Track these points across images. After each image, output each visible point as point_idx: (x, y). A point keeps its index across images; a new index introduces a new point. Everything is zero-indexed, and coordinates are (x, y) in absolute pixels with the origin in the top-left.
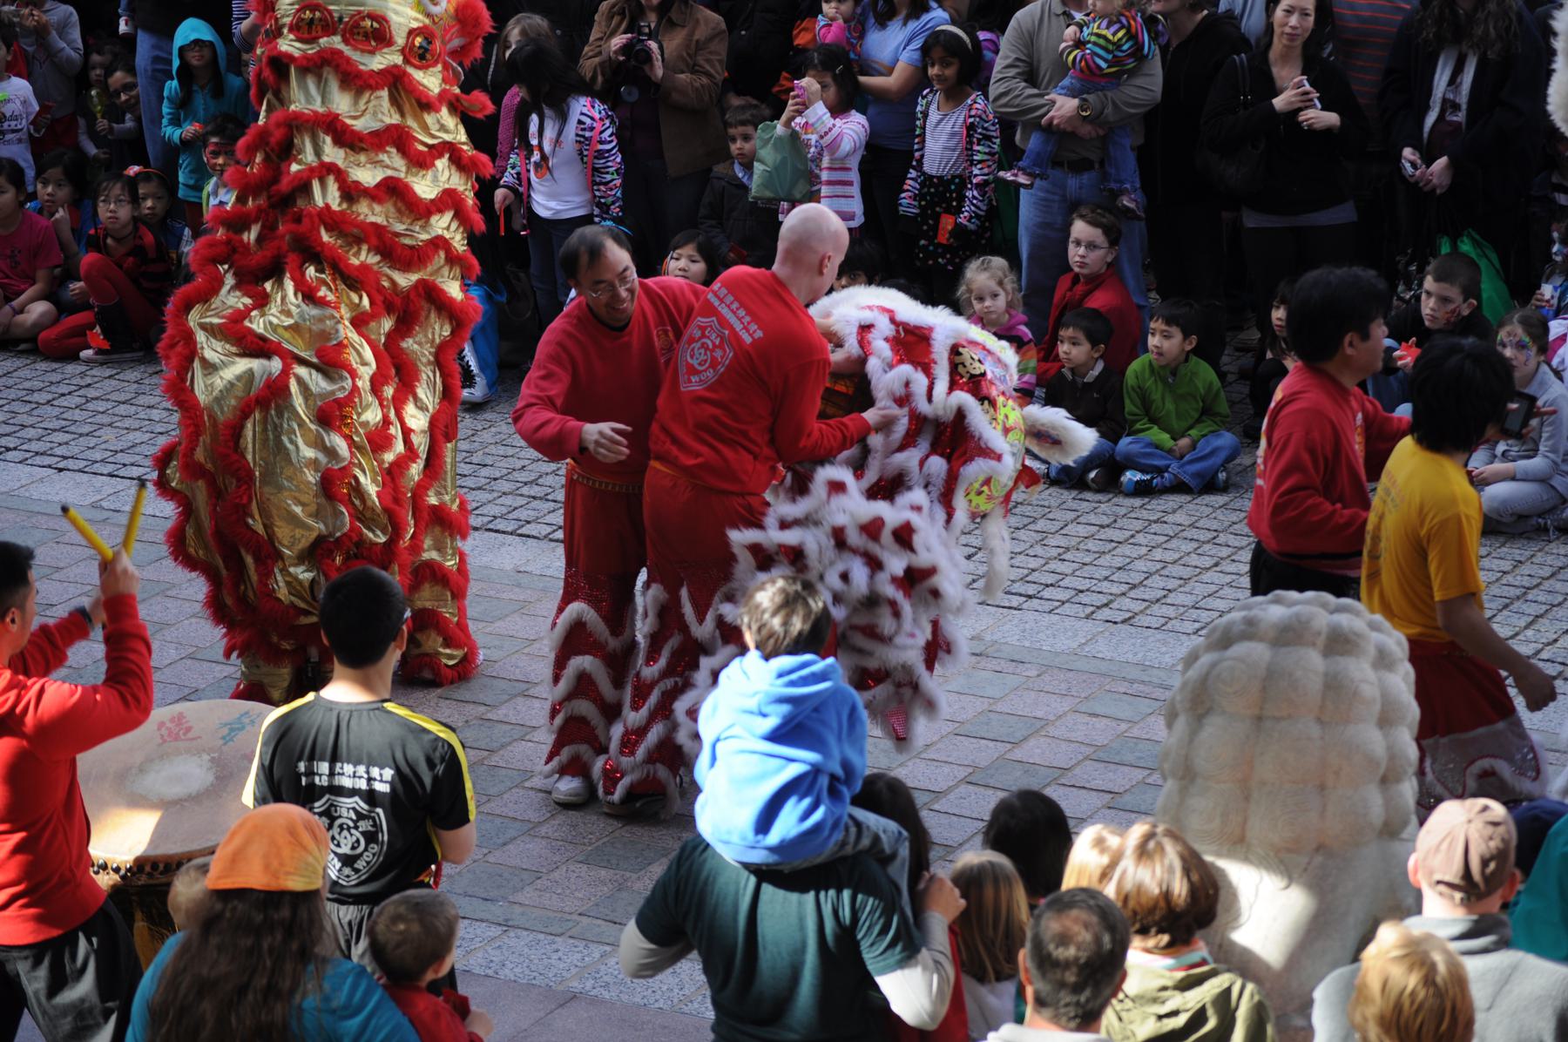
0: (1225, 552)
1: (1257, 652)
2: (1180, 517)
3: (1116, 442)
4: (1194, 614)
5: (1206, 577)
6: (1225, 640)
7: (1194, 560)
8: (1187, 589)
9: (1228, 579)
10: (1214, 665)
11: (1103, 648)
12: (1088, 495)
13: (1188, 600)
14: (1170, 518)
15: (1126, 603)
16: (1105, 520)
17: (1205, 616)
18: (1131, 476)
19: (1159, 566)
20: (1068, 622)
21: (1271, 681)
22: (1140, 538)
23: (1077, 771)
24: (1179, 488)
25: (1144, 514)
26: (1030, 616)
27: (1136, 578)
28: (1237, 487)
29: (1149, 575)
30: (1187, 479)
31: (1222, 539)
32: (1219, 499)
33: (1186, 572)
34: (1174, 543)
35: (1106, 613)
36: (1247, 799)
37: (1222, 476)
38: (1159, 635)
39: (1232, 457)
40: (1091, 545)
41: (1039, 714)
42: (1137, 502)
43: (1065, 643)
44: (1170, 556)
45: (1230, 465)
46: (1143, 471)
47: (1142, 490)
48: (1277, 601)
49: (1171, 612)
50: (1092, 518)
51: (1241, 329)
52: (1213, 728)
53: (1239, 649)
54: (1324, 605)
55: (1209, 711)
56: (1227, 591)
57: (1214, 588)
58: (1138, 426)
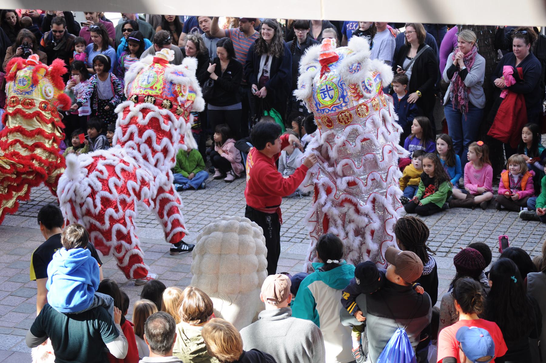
0: (206, 207)
1: (219, 234)
2: (192, 197)
4: (197, 226)
5: (200, 214)
7: (196, 210)
8: (195, 218)
9: (207, 215)
10: (206, 239)
13: (196, 222)
14: (188, 198)
17: (201, 226)
19: (186, 212)
21: (223, 244)
23: (165, 275)
24: (191, 188)
26: (148, 229)
28: (208, 187)
30: (193, 186)
31: (204, 203)
33: (194, 213)
34: (190, 205)
36: (218, 279)
37: (203, 184)
39: (206, 179)
41: (153, 258)
44: (189, 209)
45: (206, 181)
46: (180, 184)
48: (224, 219)
51: (207, 140)
52: (206, 258)
53: (213, 234)
54: (238, 220)
56: (207, 218)
57: (203, 218)
58: (178, 171)
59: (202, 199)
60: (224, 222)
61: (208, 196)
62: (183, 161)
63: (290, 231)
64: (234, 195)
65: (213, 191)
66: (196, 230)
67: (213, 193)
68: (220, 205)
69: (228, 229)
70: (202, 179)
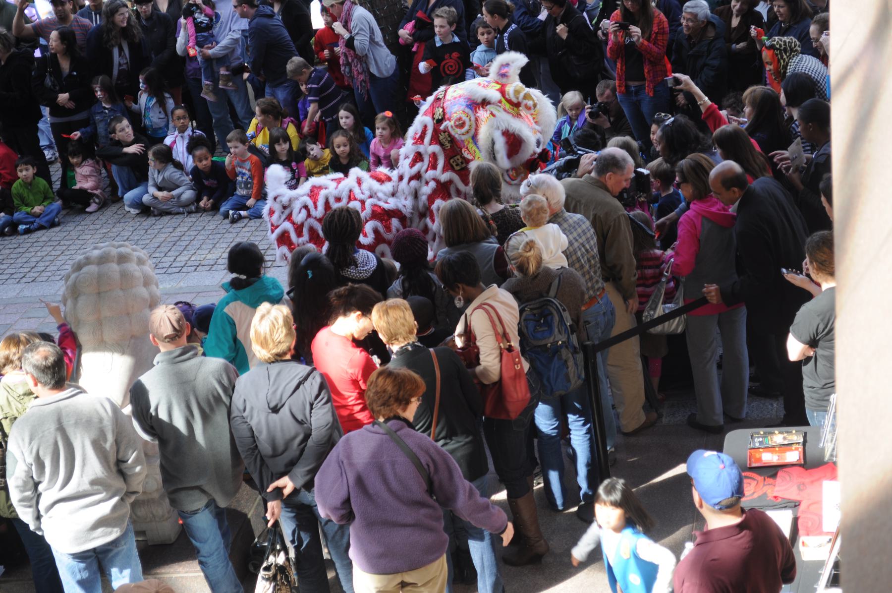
0: (64, 248)
1: (92, 268)
2: (44, 238)
3: (12, 215)
4: (59, 273)
5: (60, 258)
6: (79, 267)
10: (77, 277)
11: (27, 293)
12: (6, 238)
13: (55, 268)
14: (40, 240)
15: (31, 274)
16: (16, 246)
17: (63, 273)
18: (21, 227)
20: (10, 286)
21: (100, 278)
22: (31, 249)
24: (41, 228)
25: (30, 240)
27: (33, 264)
28: (63, 223)
29: (38, 262)
30: (43, 224)
31: (62, 243)
32: (57, 229)
33: (52, 258)
34: (44, 249)
35: (24, 280)
36: (101, 324)
37: (57, 220)
38: (47, 283)
40: (12, 256)
42: (26, 236)
43: (12, 294)
44: (44, 254)
47: (27, 232)
48: (95, 248)
49: (49, 274)
50: (10, 246)
52: (82, 301)
53: (85, 269)
55: (79, 295)
56: (69, 262)
59: (58, 239)
60: (96, 253)
61: (65, 234)
62: (25, 195)
63: (178, 259)
64: (98, 227)
65: (70, 227)
66: (58, 278)
67: (71, 228)
68: (82, 242)
69: (103, 260)
70: (54, 214)
